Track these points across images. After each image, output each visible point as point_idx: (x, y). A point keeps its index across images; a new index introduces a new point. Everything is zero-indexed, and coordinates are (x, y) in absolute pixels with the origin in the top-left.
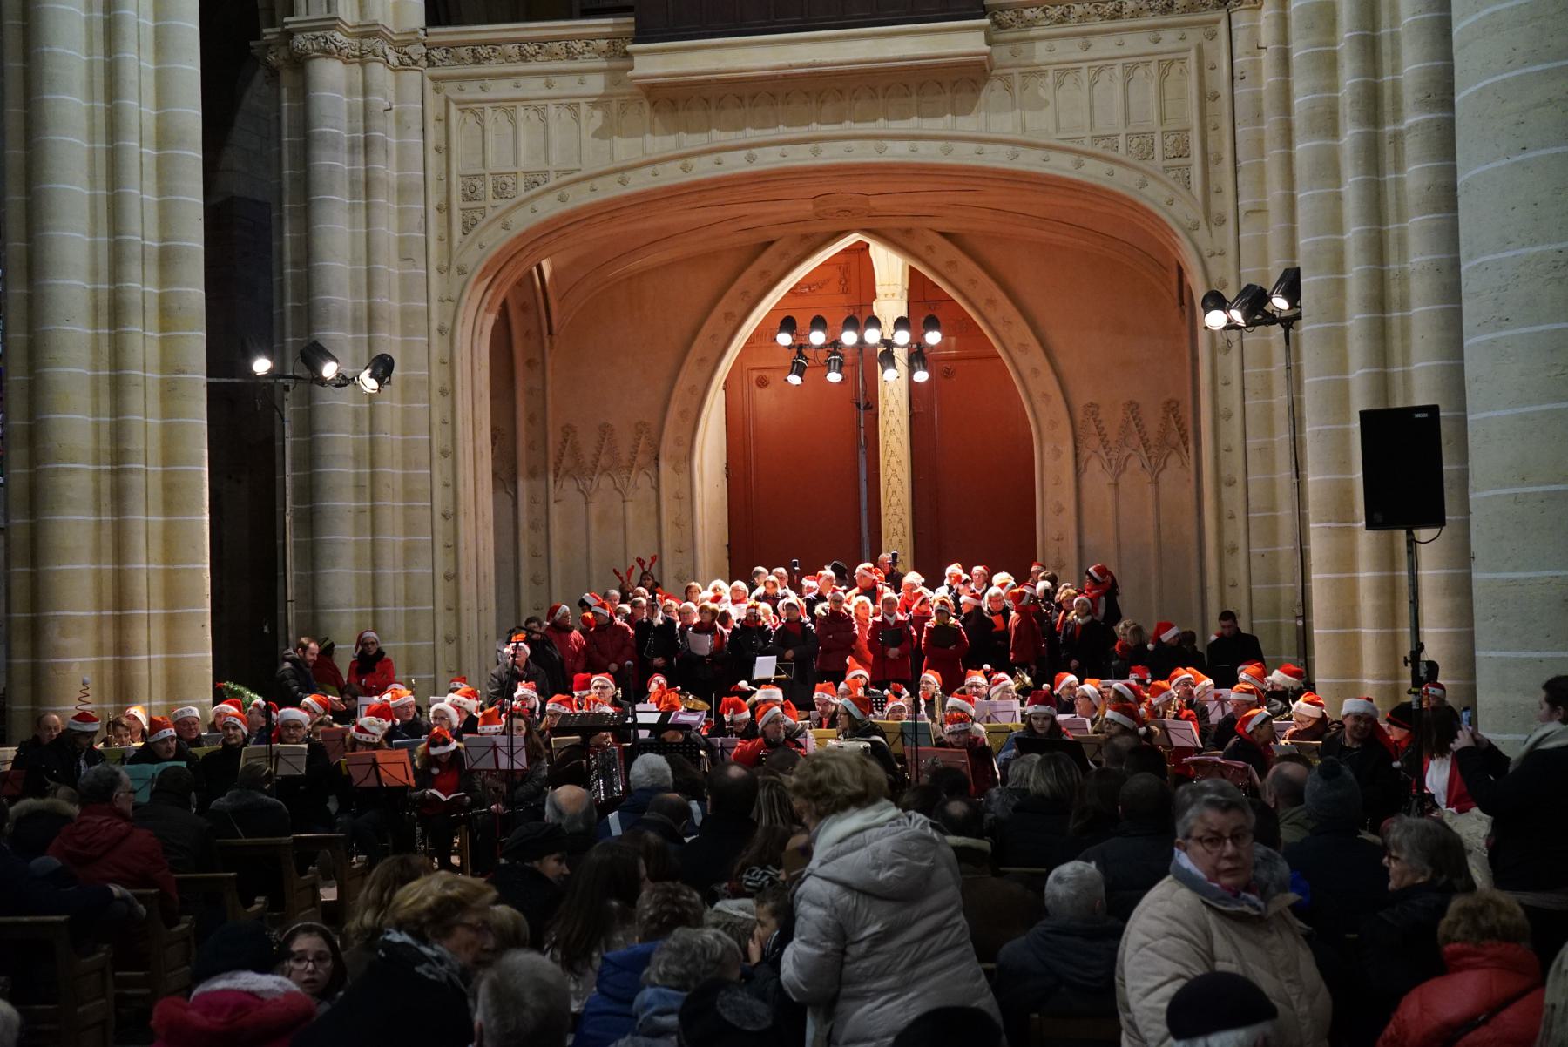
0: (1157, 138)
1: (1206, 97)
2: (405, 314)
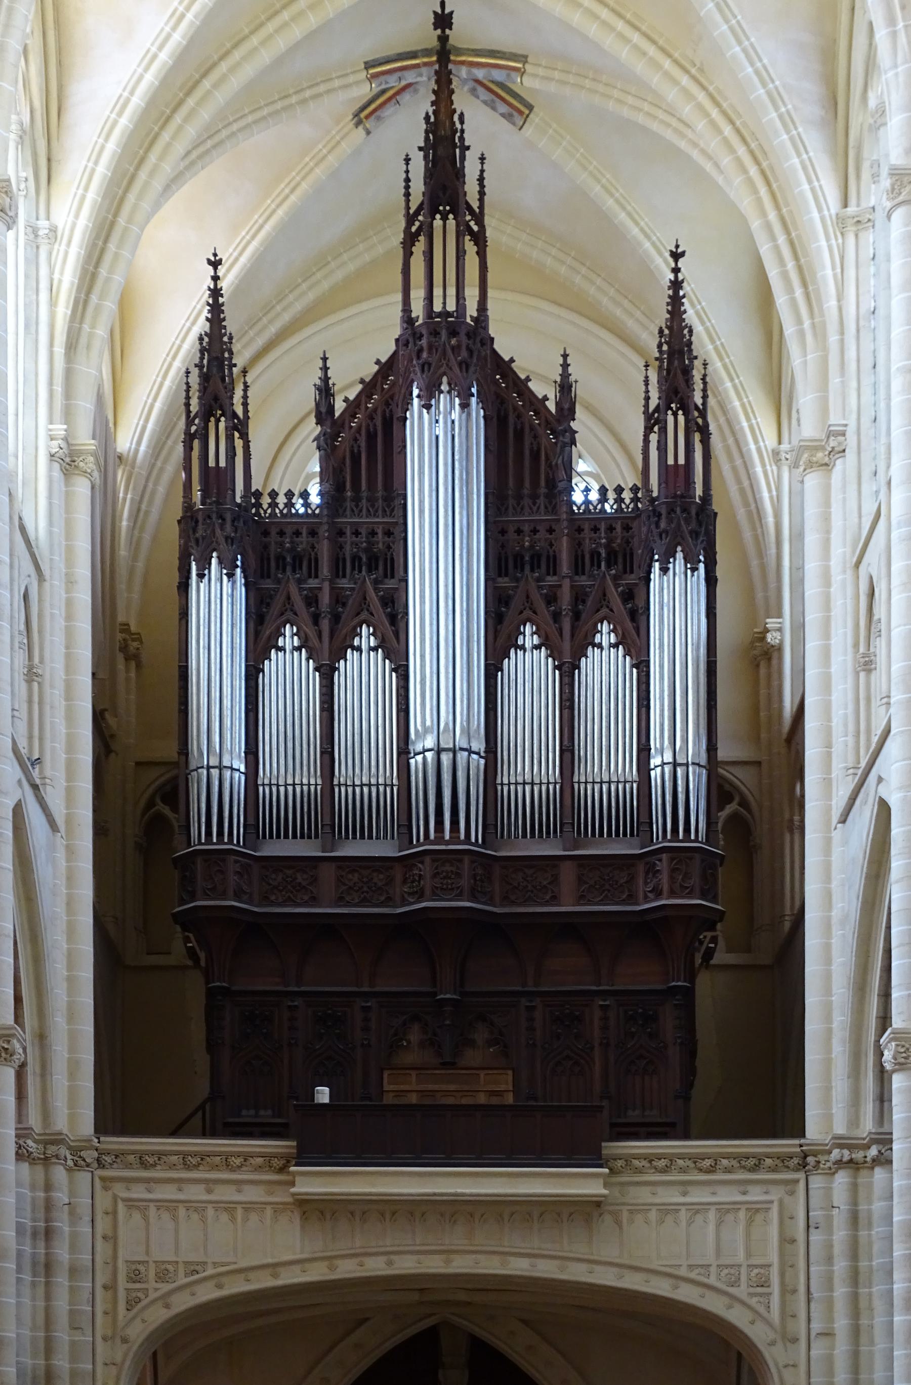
1: (787, 1241)
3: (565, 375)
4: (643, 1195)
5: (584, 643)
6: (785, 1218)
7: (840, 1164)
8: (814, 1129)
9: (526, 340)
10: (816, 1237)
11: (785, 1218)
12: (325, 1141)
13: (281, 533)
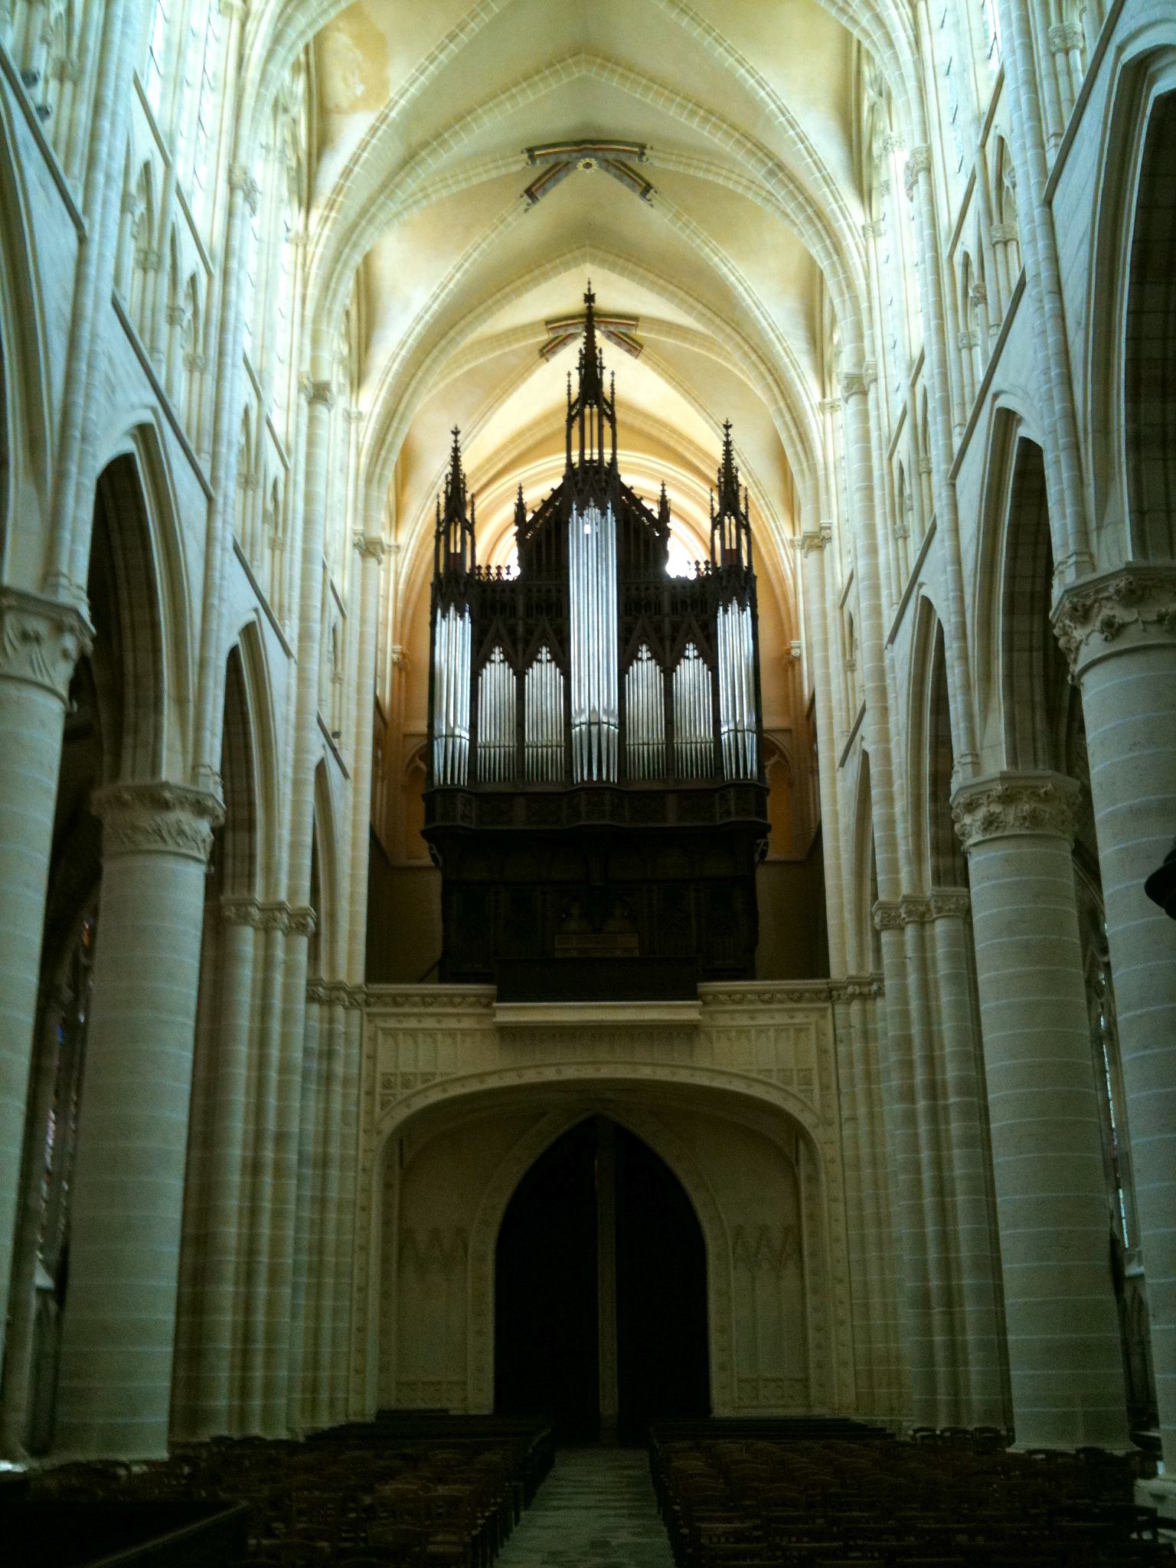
0: (795, 1073)
1: (822, 1051)
2: (343, 1158)
3: (663, 496)
4: (723, 1020)
5: (681, 655)
6: (821, 1034)
7: (853, 996)
8: (836, 972)
9: (641, 474)
10: (841, 1048)
11: (821, 1034)
12: (516, 987)
13: (494, 591)
